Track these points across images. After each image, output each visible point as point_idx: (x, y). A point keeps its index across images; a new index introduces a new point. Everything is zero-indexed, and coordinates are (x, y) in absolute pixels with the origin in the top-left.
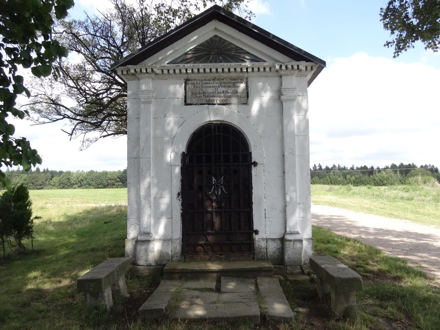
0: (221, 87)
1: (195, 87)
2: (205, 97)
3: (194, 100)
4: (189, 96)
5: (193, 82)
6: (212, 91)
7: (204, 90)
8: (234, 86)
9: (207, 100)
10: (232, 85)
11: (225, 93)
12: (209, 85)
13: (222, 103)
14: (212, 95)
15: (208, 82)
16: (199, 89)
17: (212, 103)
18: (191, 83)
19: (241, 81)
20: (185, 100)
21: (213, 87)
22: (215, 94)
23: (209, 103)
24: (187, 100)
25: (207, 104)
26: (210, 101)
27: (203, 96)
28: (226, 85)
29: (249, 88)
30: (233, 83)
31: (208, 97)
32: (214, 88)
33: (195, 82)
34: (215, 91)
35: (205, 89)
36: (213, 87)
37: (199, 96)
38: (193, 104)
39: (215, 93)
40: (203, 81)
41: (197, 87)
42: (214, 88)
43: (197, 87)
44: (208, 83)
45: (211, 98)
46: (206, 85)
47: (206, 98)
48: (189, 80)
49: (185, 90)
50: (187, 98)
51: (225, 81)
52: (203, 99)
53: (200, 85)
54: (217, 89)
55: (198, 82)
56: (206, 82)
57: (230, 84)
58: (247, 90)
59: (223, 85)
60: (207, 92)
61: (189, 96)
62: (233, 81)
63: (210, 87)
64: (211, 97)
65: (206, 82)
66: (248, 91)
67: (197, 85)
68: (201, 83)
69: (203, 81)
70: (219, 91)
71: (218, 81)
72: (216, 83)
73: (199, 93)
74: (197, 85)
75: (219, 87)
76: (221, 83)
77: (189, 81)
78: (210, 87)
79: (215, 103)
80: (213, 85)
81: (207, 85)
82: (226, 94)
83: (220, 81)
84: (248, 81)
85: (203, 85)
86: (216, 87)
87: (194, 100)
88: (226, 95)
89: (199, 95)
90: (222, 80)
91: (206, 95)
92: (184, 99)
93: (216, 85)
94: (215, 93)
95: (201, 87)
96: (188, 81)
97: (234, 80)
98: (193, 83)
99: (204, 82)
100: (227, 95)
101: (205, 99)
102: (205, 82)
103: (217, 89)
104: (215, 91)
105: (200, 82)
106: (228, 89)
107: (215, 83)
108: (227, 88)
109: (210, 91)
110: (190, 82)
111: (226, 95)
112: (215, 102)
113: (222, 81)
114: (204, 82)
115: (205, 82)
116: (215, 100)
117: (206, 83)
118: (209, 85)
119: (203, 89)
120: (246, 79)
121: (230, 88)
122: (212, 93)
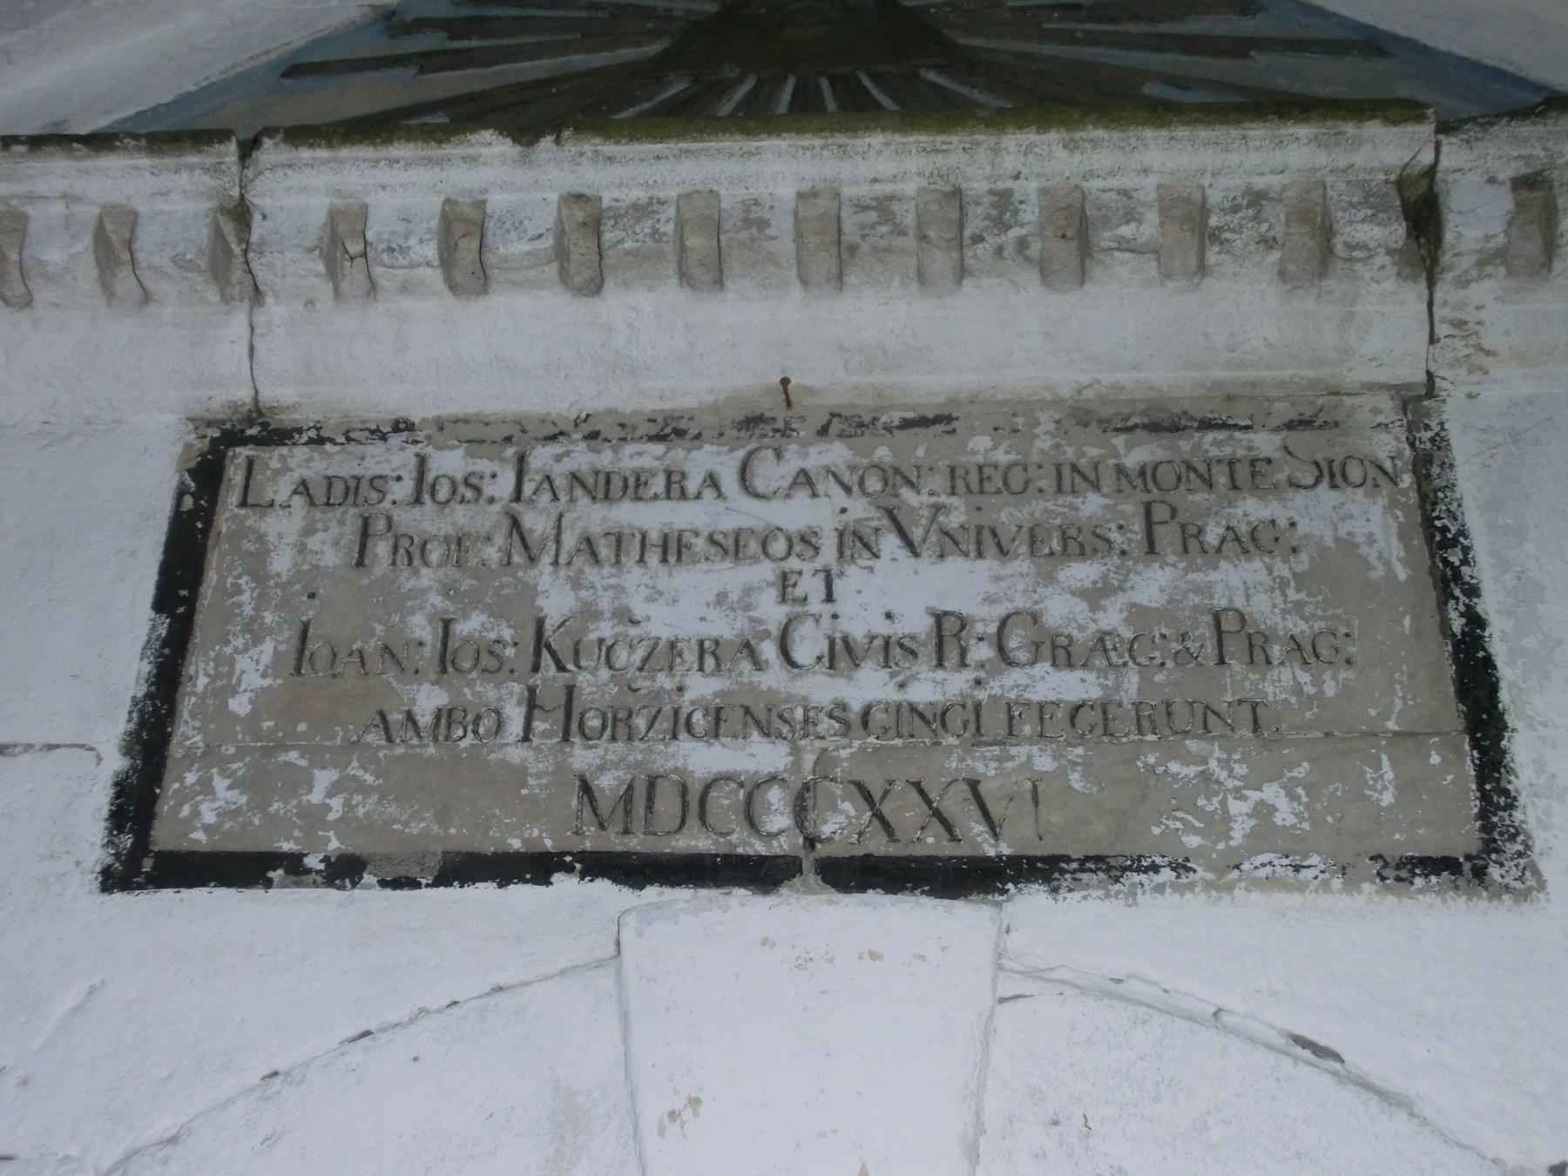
0: (890, 543)
1: (382, 549)
2: (571, 724)
3: (324, 778)
4: (240, 705)
5: (340, 463)
6: (723, 627)
7: (556, 602)
8: (1167, 536)
9: (607, 782)
10: (1131, 508)
11: (981, 652)
12: (653, 517)
13: (932, 843)
14: (702, 687)
15: (646, 457)
16: (447, 591)
17: (697, 842)
18: (303, 488)
19: (1303, 441)
20: (122, 788)
21: (732, 547)
22: (774, 678)
23: (636, 843)
24: (181, 779)
25: (597, 865)
26: (668, 805)
27: (515, 716)
28: (1008, 515)
29: (1483, 570)
30: (1148, 474)
31: (618, 724)
32: (766, 571)
33: (395, 459)
34: (772, 612)
35: (576, 584)
36: (732, 547)
37: (446, 717)
38: (294, 866)
39: (769, 650)
40: (541, 457)
41: (411, 551)
42: (766, 571)
43: (411, 551)
44: (635, 486)
45: (685, 745)
46: (591, 516)
47: (582, 757)
48: (279, 436)
49: (162, 603)
50: (188, 733)
51: (981, 443)
52: (519, 775)
53: (489, 518)
54: (811, 586)
55: (449, 462)
56: (605, 459)
57: (1091, 505)
58: (1445, 595)
59: (954, 520)
60: (606, 629)
61: (240, 705)
62: (1138, 455)
63: (674, 548)
64: (680, 725)
65: (605, 459)
66: (1475, 621)
67: (425, 521)
68: (505, 485)
69: (541, 457)
70: (860, 622)
71: (836, 453)
72: (804, 480)
73: (446, 661)
74: (425, 521)
75: (856, 542)
76: (895, 476)
77: (273, 457)
78: (674, 548)
79: (759, 848)
80: (741, 513)
81: (627, 514)
82: (1016, 676)
83: (883, 454)
84: (1440, 441)
85: (537, 522)
86: (807, 541)
87: (324, 778)
88: (1009, 683)
89: (428, 699)
90: (923, 422)
91: (593, 683)
92: (115, 762)
93: (797, 513)
94: (769, 650)
95: (492, 553)
96: (258, 441)
97: (1154, 428)
98: (353, 489)
99: (560, 471)
100: (1039, 694)
101: (561, 770)
102: (582, 458)
103: (811, 586)
104: (772, 612)
105: (484, 466)
106: (1050, 579)
107: (769, 473)
108: (1021, 565)
109: (661, 623)
110: (301, 462)
111: (1009, 683)
112: (778, 819)
113: (920, 447)
114: (560, 471)
115: (582, 458)
116: (775, 795)
117: (603, 487)
118: (653, 517)
119: (530, 592)
120: (1385, 403)
121: (1082, 572)
122: (710, 652)
